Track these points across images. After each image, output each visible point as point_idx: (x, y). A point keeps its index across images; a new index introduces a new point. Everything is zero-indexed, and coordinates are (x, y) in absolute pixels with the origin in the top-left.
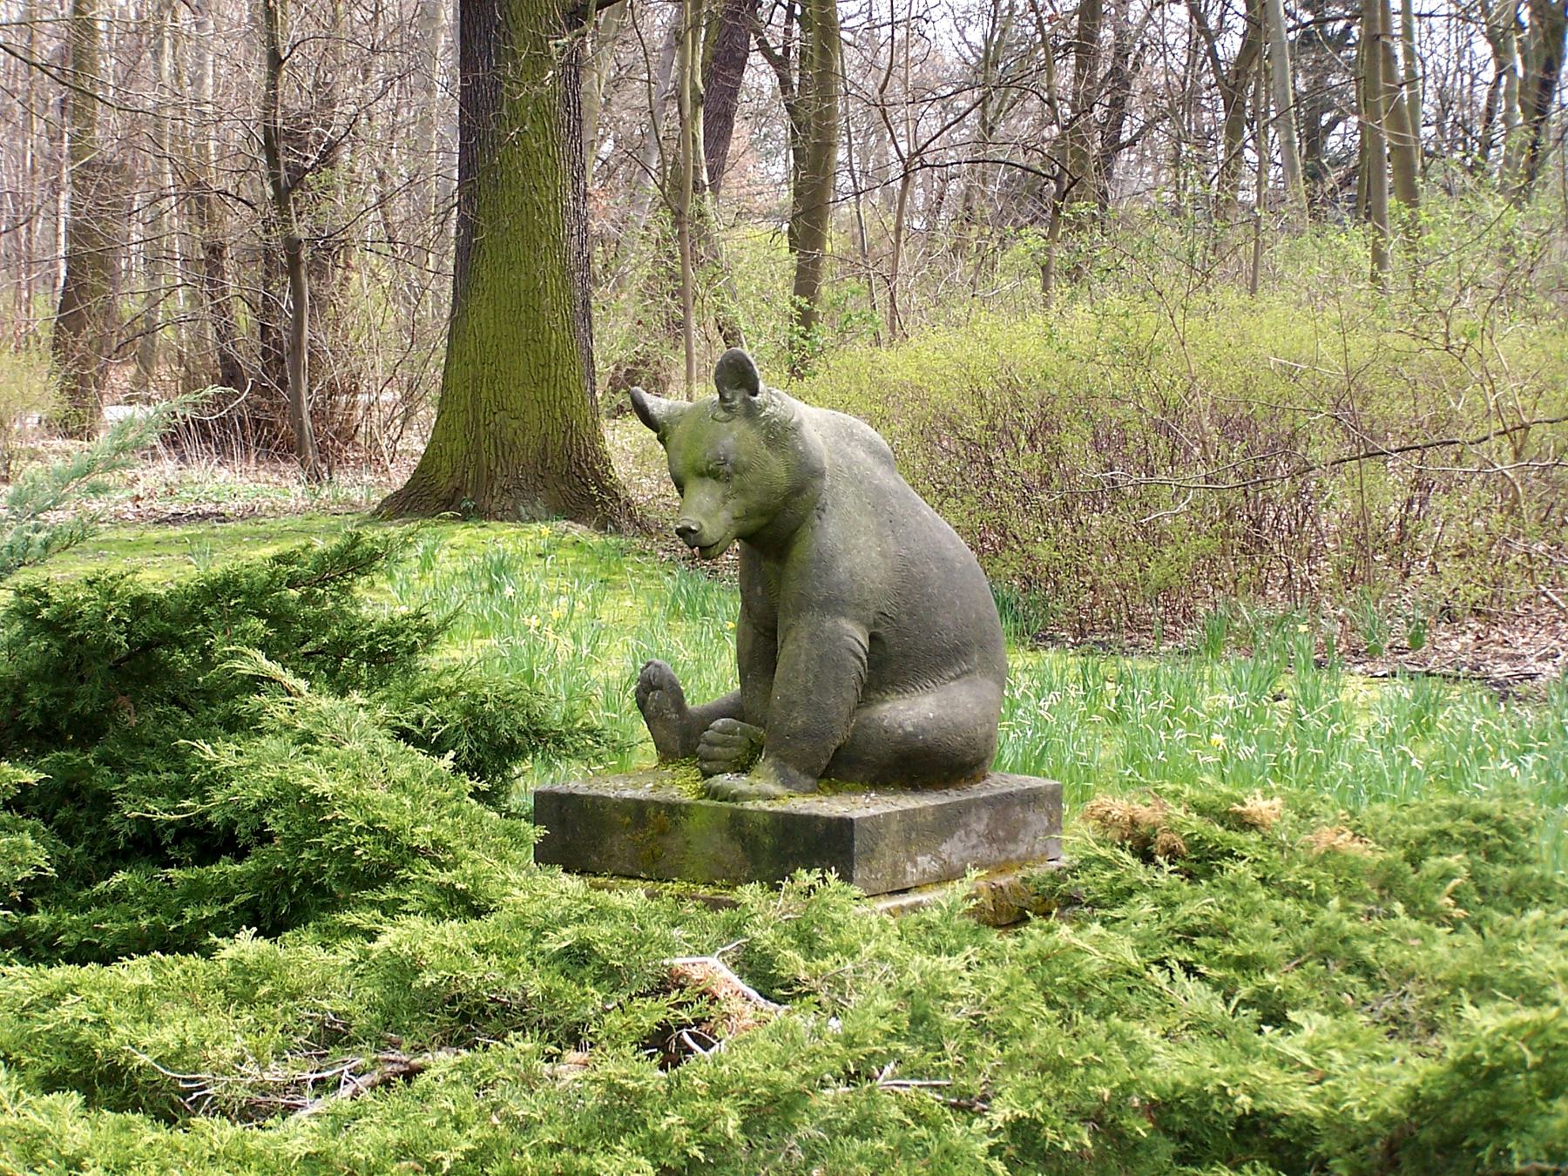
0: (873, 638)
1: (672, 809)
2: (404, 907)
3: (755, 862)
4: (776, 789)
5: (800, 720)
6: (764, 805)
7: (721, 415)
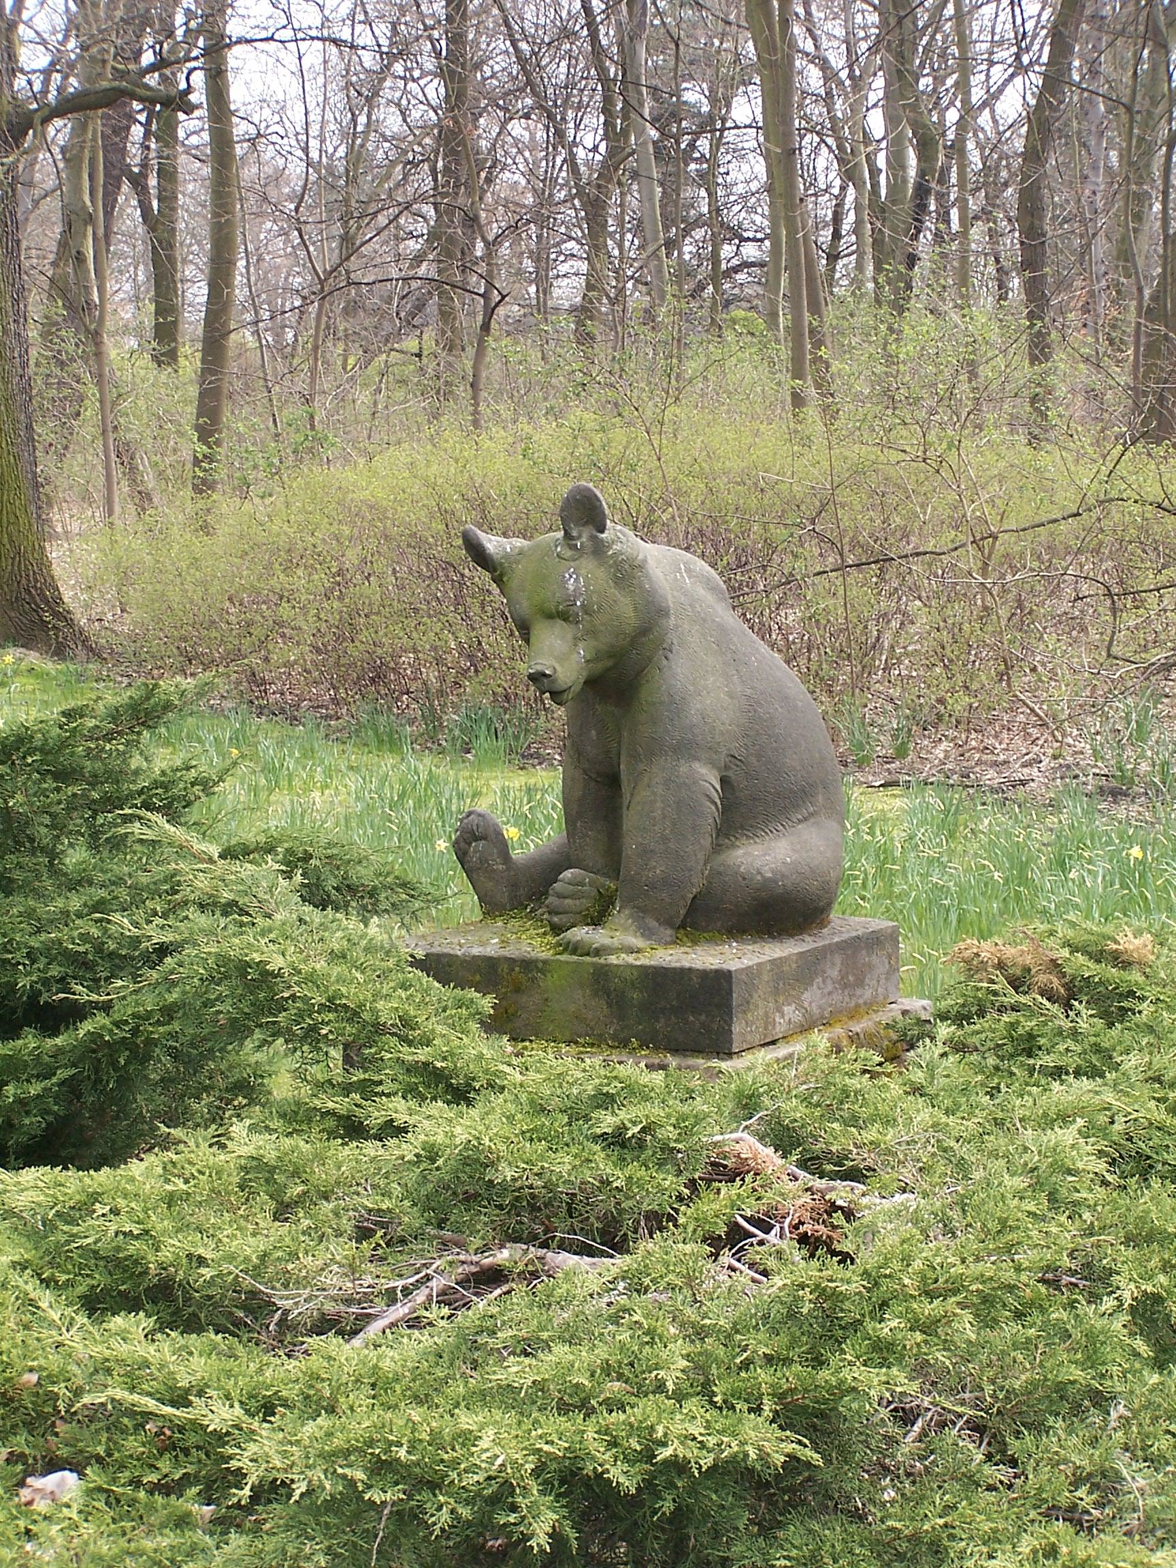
0: (724, 781)
1: (528, 965)
2: (379, 1089)
3: (621, 1018)
4: (638, 942)
5: (658, 869)
6: (630, 959)
7: (568, 553)
